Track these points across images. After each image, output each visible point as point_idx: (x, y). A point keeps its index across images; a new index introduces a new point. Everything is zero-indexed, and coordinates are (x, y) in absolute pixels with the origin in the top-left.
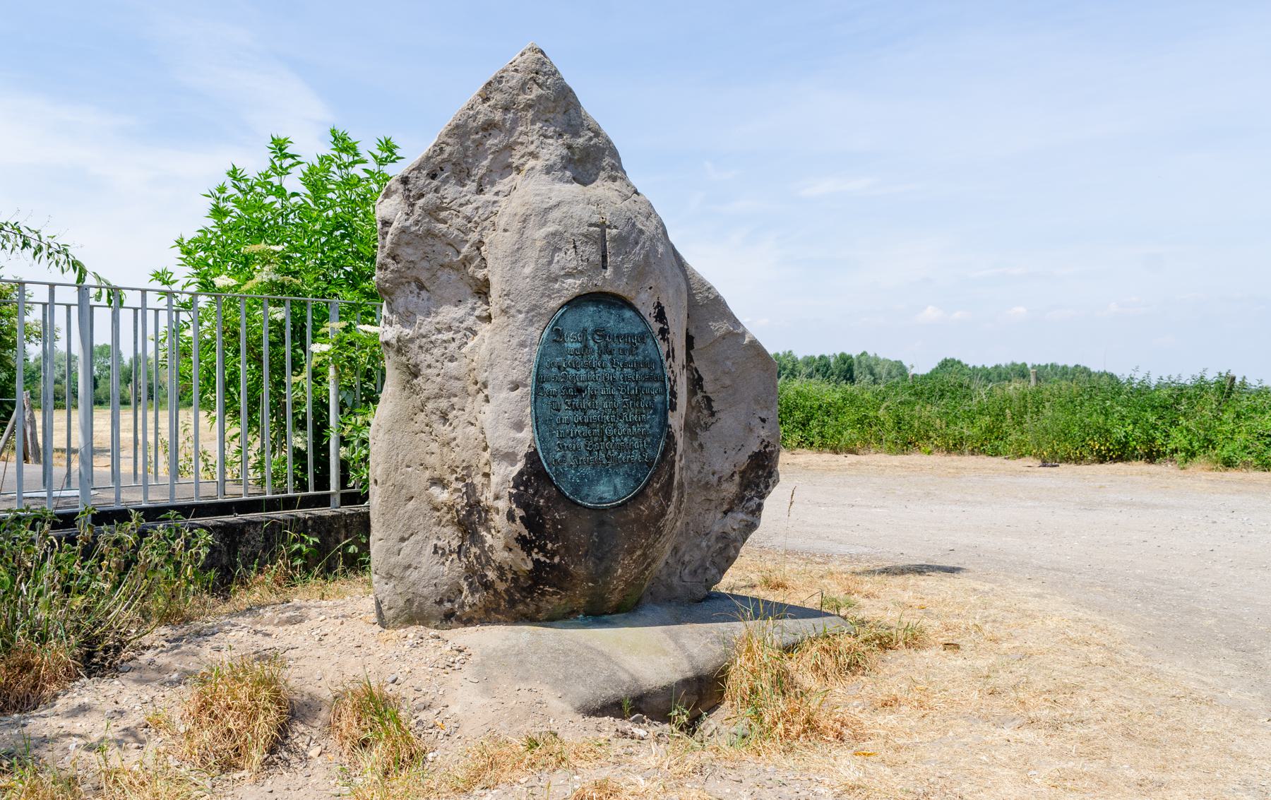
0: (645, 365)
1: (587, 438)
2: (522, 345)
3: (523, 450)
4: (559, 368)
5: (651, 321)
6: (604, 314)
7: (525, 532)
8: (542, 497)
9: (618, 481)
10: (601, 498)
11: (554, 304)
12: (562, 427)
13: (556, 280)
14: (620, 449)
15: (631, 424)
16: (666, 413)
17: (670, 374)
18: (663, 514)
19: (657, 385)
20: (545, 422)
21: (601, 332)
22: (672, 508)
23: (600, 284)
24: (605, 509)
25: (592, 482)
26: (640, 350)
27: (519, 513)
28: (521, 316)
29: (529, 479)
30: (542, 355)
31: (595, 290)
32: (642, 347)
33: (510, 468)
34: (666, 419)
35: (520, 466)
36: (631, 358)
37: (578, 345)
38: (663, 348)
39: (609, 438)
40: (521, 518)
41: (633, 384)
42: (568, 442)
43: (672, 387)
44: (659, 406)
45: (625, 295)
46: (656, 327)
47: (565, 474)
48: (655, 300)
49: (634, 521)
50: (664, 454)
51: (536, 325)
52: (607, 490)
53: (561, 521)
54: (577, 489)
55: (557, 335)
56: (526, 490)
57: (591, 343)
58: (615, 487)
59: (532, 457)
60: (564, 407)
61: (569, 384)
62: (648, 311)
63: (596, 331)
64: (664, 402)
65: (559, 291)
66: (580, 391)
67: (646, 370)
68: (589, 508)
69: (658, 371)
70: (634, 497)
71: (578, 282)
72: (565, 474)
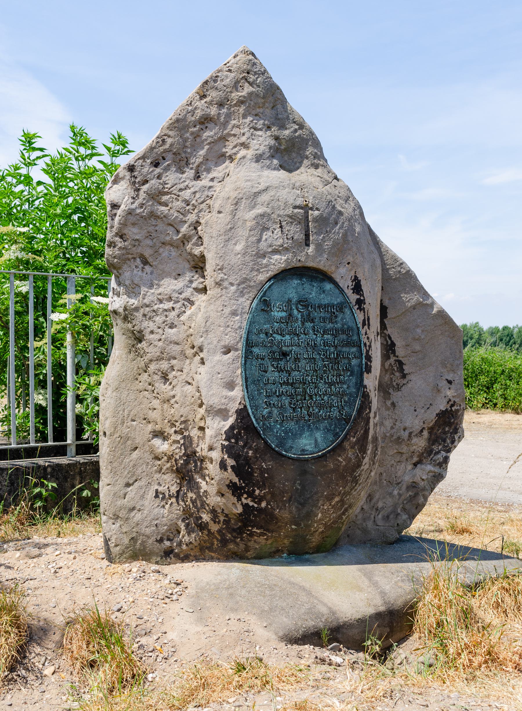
0: (343, 332)
1: (291, 396)
2: (234, 313)
3: (234, 407)
4: (266, 334)
5: (349, 292)
6: (307, 286)
7: (236, 480)
8: (250, 448)
9: (319, 435)
10: (303, 450)
11: (262, 277)
12: (269, 387)
13: (264, 256)
14: (321, 407)
15: (330, 384)
16: (362, 375)
17: (366, 340)
18: (359, 465)
19: (354, 349)
20: (253, 382)
21: (304, 302)
22: (366, 460)
23: (303, 259)
24: (307, 460)
25: (296, 436)
26: (339, 319)
27: (231, 462)
28: (233, 288)
29: (239, 433)
30: (251, 323)
31: (299, 265)
32: (340, 316)
33: (223, 423)
34: (362, 380)
35: (231, 421)
36: (331, 325)
37: (284, 314)
38: (360, 317)
39: (311, 397)
40: (232, 467)
41: (332, 349)
42: (274, 400)
43: (368, 352)
44: (356, 369)
45: (325, 269)
46: (353, 298)
47: (271, 429)
48: (352, 273)
49: (333, 471)
50: (360, 411)
51: (246, 296)
52: (309, 443)
53: (267, 470)
54: (281, 443)
56: (237, 442)
57: (295, 312)
58: (316, 441)
59: (242, 413)
60: (271, 369)
61: (275, 348)
62: (346, 284)
63: (299, 302)
64: (360, 365)
65: (267, 266)
66: (285, 354)
67: (345, 337)
68: (292, 459)
69: (355, 338)
70: (333, 450)
71: (284, 258)
72: (271, 429)
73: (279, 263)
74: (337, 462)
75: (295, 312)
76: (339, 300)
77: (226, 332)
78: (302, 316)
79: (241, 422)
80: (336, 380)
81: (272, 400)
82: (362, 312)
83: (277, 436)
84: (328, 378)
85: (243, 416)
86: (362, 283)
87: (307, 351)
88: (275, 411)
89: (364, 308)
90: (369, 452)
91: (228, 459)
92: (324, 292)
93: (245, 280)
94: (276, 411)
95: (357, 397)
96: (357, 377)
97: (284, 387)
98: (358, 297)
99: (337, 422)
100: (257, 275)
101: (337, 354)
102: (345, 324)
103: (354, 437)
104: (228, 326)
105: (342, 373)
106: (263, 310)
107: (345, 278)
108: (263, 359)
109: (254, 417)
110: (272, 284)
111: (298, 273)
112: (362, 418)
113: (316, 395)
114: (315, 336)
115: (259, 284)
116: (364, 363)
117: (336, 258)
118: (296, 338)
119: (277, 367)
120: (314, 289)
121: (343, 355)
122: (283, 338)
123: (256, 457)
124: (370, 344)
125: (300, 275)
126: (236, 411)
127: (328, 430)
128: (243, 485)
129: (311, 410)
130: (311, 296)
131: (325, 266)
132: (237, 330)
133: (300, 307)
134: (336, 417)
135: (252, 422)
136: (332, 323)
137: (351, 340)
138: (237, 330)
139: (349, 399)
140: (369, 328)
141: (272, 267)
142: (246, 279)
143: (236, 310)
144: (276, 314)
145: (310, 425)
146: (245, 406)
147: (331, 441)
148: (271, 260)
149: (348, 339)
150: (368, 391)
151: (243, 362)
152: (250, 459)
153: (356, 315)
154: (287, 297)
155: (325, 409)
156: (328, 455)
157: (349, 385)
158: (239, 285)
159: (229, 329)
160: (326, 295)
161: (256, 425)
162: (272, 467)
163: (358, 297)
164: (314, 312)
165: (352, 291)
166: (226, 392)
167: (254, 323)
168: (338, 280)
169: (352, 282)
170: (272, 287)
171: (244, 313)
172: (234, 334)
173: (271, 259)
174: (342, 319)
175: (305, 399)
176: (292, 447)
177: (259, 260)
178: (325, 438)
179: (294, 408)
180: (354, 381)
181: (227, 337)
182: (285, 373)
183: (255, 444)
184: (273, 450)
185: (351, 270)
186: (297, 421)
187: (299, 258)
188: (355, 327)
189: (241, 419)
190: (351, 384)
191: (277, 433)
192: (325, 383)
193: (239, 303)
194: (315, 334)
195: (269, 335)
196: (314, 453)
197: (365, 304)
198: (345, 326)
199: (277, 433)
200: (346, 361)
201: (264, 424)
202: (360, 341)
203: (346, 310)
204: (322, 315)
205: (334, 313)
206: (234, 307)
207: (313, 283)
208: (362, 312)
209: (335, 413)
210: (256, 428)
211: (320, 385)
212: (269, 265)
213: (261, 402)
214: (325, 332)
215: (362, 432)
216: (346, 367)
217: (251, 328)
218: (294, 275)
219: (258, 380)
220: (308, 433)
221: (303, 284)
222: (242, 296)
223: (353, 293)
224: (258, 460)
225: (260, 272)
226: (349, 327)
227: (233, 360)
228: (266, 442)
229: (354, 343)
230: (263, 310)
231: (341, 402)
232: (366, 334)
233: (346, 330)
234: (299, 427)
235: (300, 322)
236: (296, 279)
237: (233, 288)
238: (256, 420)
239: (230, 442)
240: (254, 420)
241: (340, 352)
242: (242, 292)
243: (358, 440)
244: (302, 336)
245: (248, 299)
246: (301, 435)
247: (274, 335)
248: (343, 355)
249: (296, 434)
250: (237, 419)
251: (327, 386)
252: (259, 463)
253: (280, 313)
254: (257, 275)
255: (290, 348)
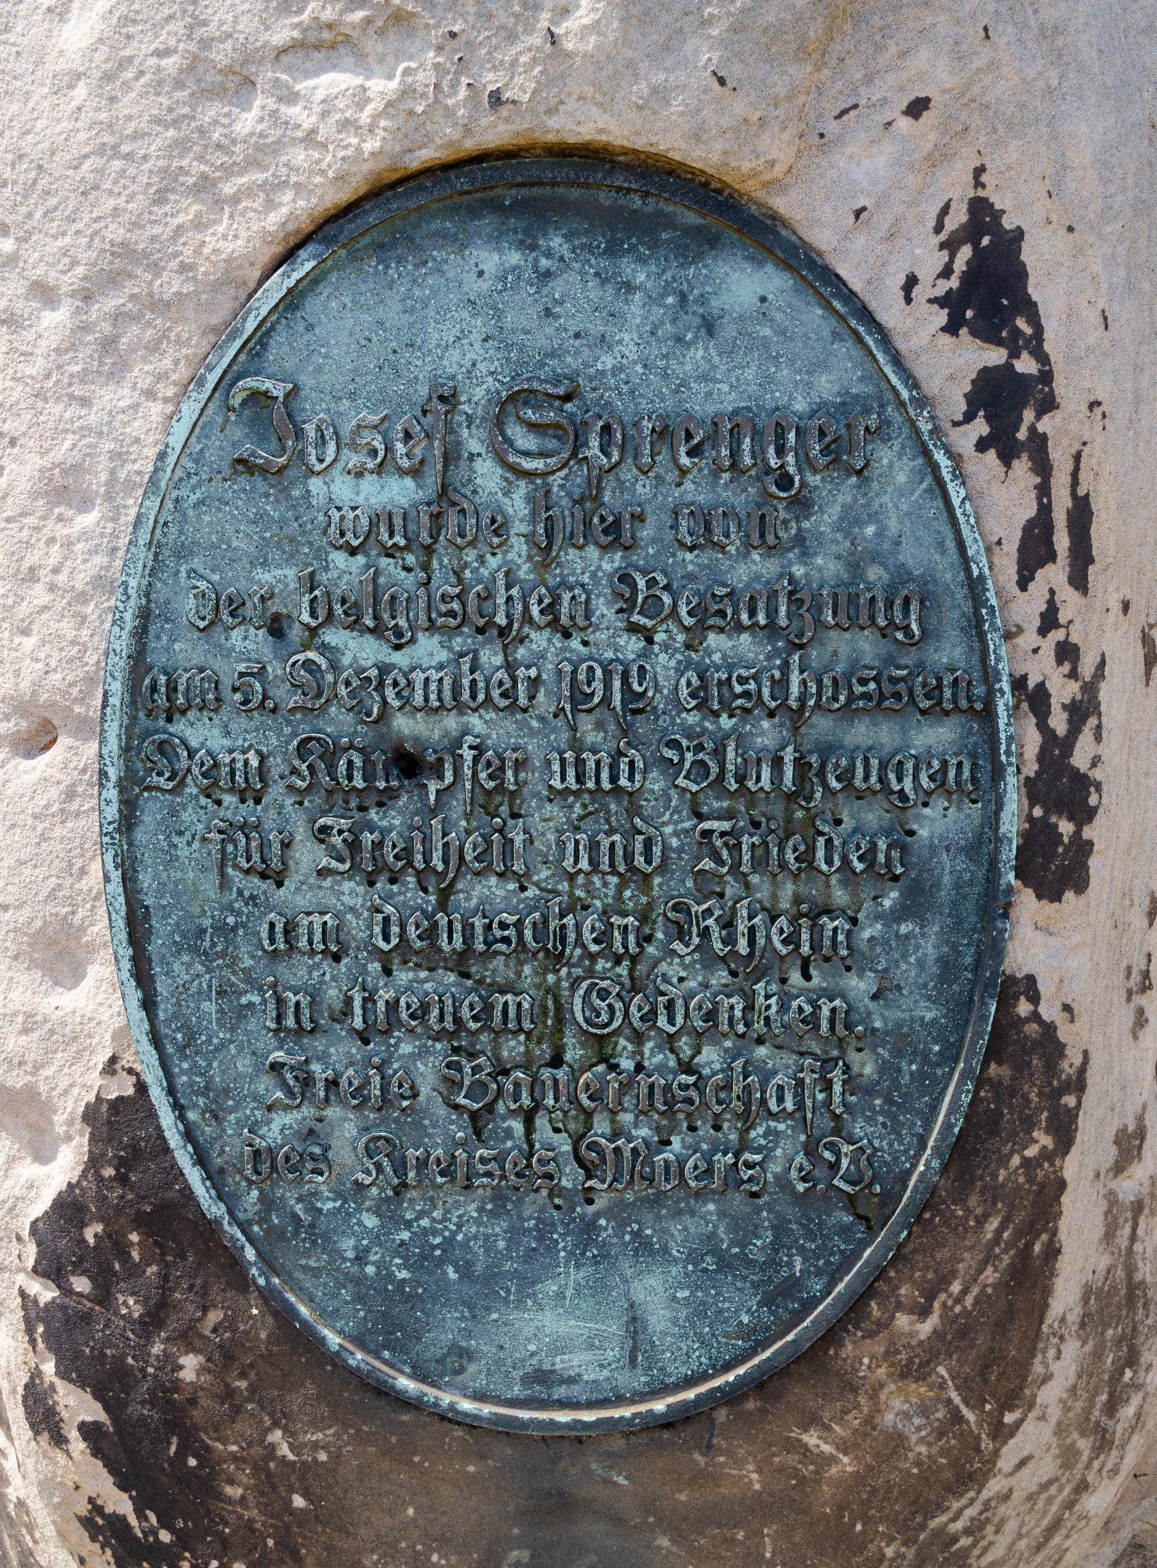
0: (853, 608)
1: (454, 1034)
2: (63, 490)
3: (78, 1085)
4: (276, 627)
5: (919, 328)
6: (578, 290)
7: (121, 1503)
8: (188, 1339)
9: (656, 1292)
10: (542, 1377)
11: (241, 234)
12: (298, 972)
13: (238, 83)
14: (669, 1108)
15: (750, 968)
16: (994, 909)
17: (1042, 668)
18: (966, 1469)
19: (938, 737)
20: (192, 941)
21: (553, 408)
22: (1033, 1440)
23: (520, 89)
24: (578, 1439)
25: (487, 1288)
26: (824, 520)
27: (78, 1406)
28: (55, 320)
29: (114, 1242)
30: (163, 552)
31: (494, 133)
32: (835, 498)
33: (28, 1170)
34: (993, 948)
35: (64, 1167)
36: (759, 567)
37: (400, 492)
38: (1004, 501)
39: (601, 1049)
40: (89, 1431)
41: (766, 733)
42: (338, 1054)
43: (1056, 751)
44: (949, 869)
45: (703, 156)
46: (949, 364)
47: (317, 1234)
48: (955, 186)
49: (760, 1509)
50: (966, 1154)
51: (141, 373)
52: (582, 1335)
53: (303, 1474)
54: (392, 1320)
55: (257, 421)
56: (103, 1295)
57: (487, 476)
58: (635, 1324)
59: (119, 1125)
60: (308, 855)
61: (339, 722)
62: (896, 260)
63: (512, 401)
64: (982, 845)
65: (262, 151)
66: (409, 764)
67: (866, 646)
68: (470, 1424)
69: (949, 652)
70: (762, 1384)
71: (382, 87)
72: (317, 1234)
73: (346, 124)
74: (792, 1459)
75: (487, 476)
76: (826, 386)
77: (24, 609)
78: (542, 502)
79: (122, 1179)
80: (791, 940)
81: (323, 1058)
82: (1022, 466)
83: (359, 1281)
84: (728, 924)
85: (134, 1148)
86: (1033, 255)
87: (577, 745)
88: (346, 1129)
89: (1039, 442)
90: (1050, 1395)
91: (58, 1382)
92: (709, 326)
93: (120, 264)
94: (350, 1129)
95: (950, 1056)
96: (958, 926)
97: (403, 976)
98: (995, 356)
99: (792, 1212)
100: (199, 224)
101: (801, 764)
102: (875, 558)
103: (924, 1312)
104: (32, 575)
105: (840, 896)
106: (243, 464)
107: (882, 223)
108: (252, 794)
109: (201, 1159)
110: (313, 281)
111: (508, 197)
112: (993, 1194)
113: (638, 1038)
114: (632, 645)
115: (217, 286)
116: (1011, 823)
117: (801, 72)
118: (491, 657)
119: (354, 846)
120: (635, 307)
121: (846, 777)
122: (400, 659)
123: (230, 1393)
124: (1091, 689)
125: (519, 207)
126: (90, 1115)
127: (725, 1264)
128: (165, 1536)
129: (601, 1125)
130: (607, 362)
131: (697, 137)
132: (82, 598)
133: (524, 440)
134: (783, 1181)
135: (188, 1193)
136: (770, 550)
137: (920, 667)
138: (82, 598)
139: (885, 1068)
140: (1079, 581)
141: (300, 156)
142: (124, 250)
143: (76, 469)
144: (343, 489)
145: (590, 1227)
146: (142, 1088)
147: (745, 1332)
148: (293, 112)
149: (890, 660)
150: (1049, 1011)
151: (112, 812)
152: (193, 1402)
153: (956, 493)
154: (421, 368)
155: (705, 1130)
156: (722, 1415)
157: (896, 974)
158: (88, 297)
159: (39, 595)
160: (727, 352)
161: (214, 1209)
162: (336, 1457)
163: (995, 356)
164: (628, 473)
165: (941, 317)
166: (25, 991)
167: (182, 553)
168: (823, 236)
169: (950, 246)
170: (313, 306)
171: (129, 486)
172: (66, 627)
173: (291, 98)
174: (849, 522)
175: (556, 1061)
176: (467, 1355)
177: (211, 111)
178: (700, 1311)
179: (474, 1116)
180: (930, 948)
181: (29, 643)
182: (409, 892)
183: (215, 1316)
184: (336, 1359)
185: (937, 159)
186: (499, 1197)
187: (491, 80)
188: (948, 575)
189: (121, 1164)
190: (906, 971)
191: (361, 1258)
192: (710, 960)
193: (93, 417)
194: (633, 628)
195: (295, 633)
196: (620, 1400)
197: (1048, 405)
198: (875, 573)
199: (361, 1258)
200: (874, 816)
201: (268, 1203)
202: (989, 676)
203: (885, 455)
204: (693, 491)
205: (785, 482)
206: (63, 451)
207: (628, 268)
208: (1022, 466)
209: (783, 1154)
210: (208, 1229)
211: (673, 969)
212: (277, 148)
213: (244, 1065)
214: (712, 614)
215: (990, 1276)
216: (868, 857)
217: (162, 592)
218: (474, 212)
219: (221, 929)
220: (576, 1276)
221: (547, 276)
222: (116, 375)
223: (951, 328)
224: (237, 1409)
225: (219, 202)
226: (901, 576)
227: (70, 794)
228: (283, 1315)
229: (934, 693)
230: (243, 464)
231: (828, 1087)
232: (1049, 621)
233: (893, 604)
234: (515, 1234)
235: (518, 549)
236: (495, 241)
237: (55, 320)
238: (214, 1177)
239: (67, 1291)
240: (194, 1176)
241: (826, 750)
242: (108, 344)
243: (956, 1335)
244: (539, 640)
245: (150, 394)
246: (527, 1283)
247: (332, 636)
248: (846, 777)
249: (491, 1278)
250: (93, 1163)
251: (721, 977)
252: (244, 1427)
253: (369, 483)
254: (199, 224)
255: (452, 722)
